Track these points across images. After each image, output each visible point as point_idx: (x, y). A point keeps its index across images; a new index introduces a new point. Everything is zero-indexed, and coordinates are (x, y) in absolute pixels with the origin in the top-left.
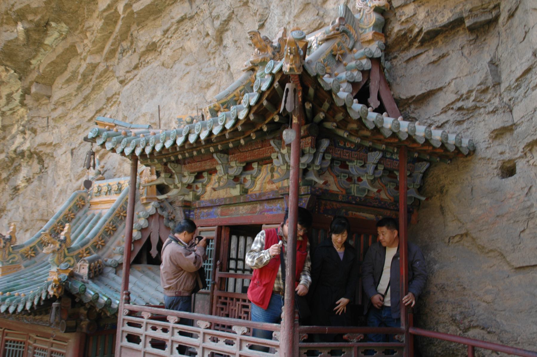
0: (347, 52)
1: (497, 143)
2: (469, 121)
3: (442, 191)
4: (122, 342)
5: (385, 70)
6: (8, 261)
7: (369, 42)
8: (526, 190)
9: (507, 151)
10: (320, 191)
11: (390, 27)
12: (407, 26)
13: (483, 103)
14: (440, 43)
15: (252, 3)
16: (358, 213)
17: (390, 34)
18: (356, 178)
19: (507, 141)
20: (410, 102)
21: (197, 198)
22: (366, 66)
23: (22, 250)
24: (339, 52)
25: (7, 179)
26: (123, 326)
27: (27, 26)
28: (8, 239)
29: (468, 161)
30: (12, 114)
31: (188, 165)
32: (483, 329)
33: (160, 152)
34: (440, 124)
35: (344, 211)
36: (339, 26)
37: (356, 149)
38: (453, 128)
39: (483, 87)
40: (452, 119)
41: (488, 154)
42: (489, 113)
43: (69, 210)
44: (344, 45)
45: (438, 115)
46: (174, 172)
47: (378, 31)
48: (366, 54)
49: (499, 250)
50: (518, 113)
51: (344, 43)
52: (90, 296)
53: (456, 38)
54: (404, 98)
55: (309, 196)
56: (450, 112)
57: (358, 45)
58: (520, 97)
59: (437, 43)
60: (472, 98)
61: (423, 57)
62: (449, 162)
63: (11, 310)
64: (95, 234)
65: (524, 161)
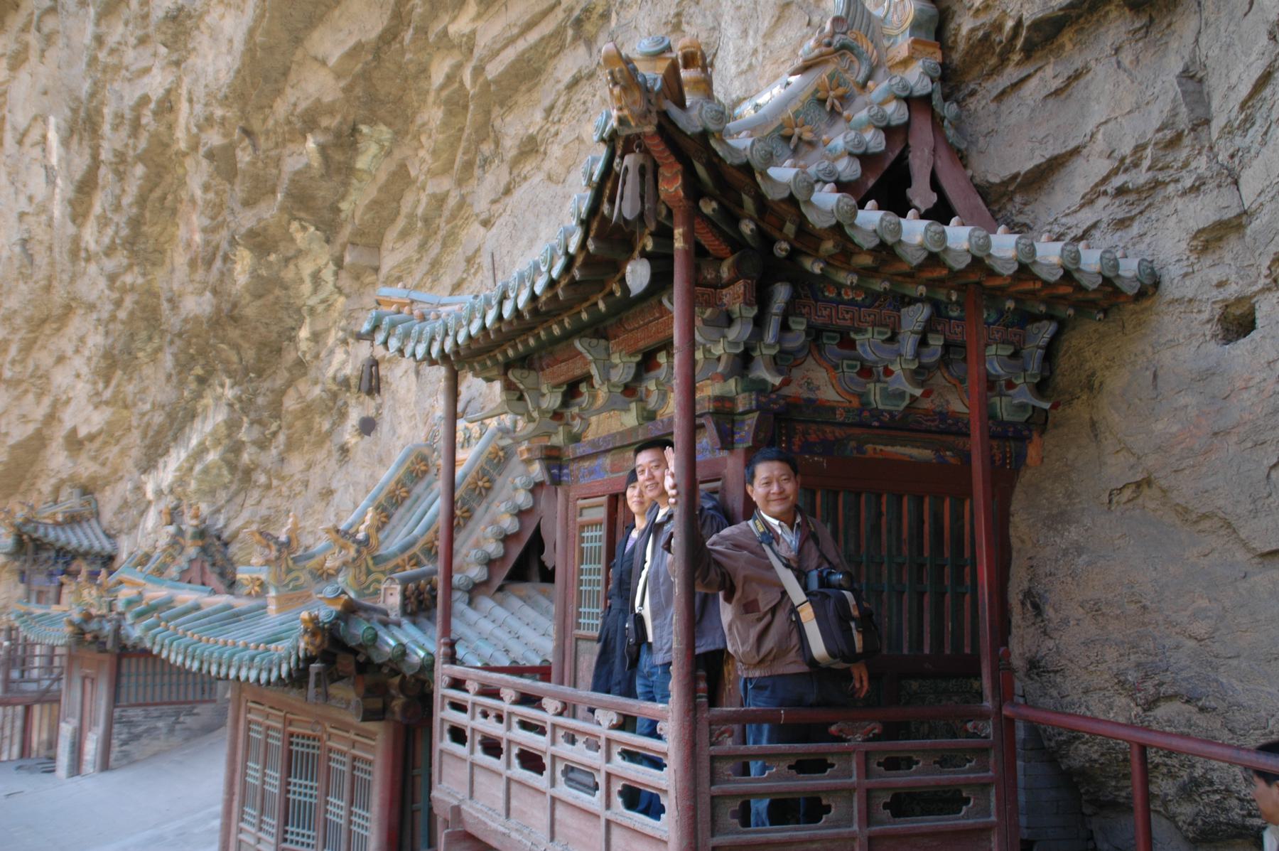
0: (856, 90)
1: (1209, 262)
2: (1143, 218)
3: (1091, 386)
5: (946, 123)
7: (905, 63)
9: (1233, 277)
10: (782, 402)
11: (952, 26)
12: (986, 19)
13: (1172, 171)
16: (889, 449)
17: (955, 42)
18: (881, 369)
19: (1231, 255)
20: (1011, 188)
21: (576, 439)
22: (895, 116)
24: (832, 93)
29: (1144, 311)
31: (548, 371)
33: (468, 347)
34: (1080, 232)
35: (853, 444)
36: (832, 36)
37: (868, 301)
38: (1108, 237)
39: (1169, 134)
40: (1105, 217)
41: (1189, 289)
42: (1184, 193)
44: (847, 76)
45: (1075, 212)
46: (522, 387)
47: (923, 39)
48: (894, 89)
50: (1251, 182)
51: (846, 71)
54: (996, 180)
55: (756, 415)
56: (1102, 201)
57: (880, 74)
58: (1256, 145)
60: (1146, 163)
62: (1101, 316)
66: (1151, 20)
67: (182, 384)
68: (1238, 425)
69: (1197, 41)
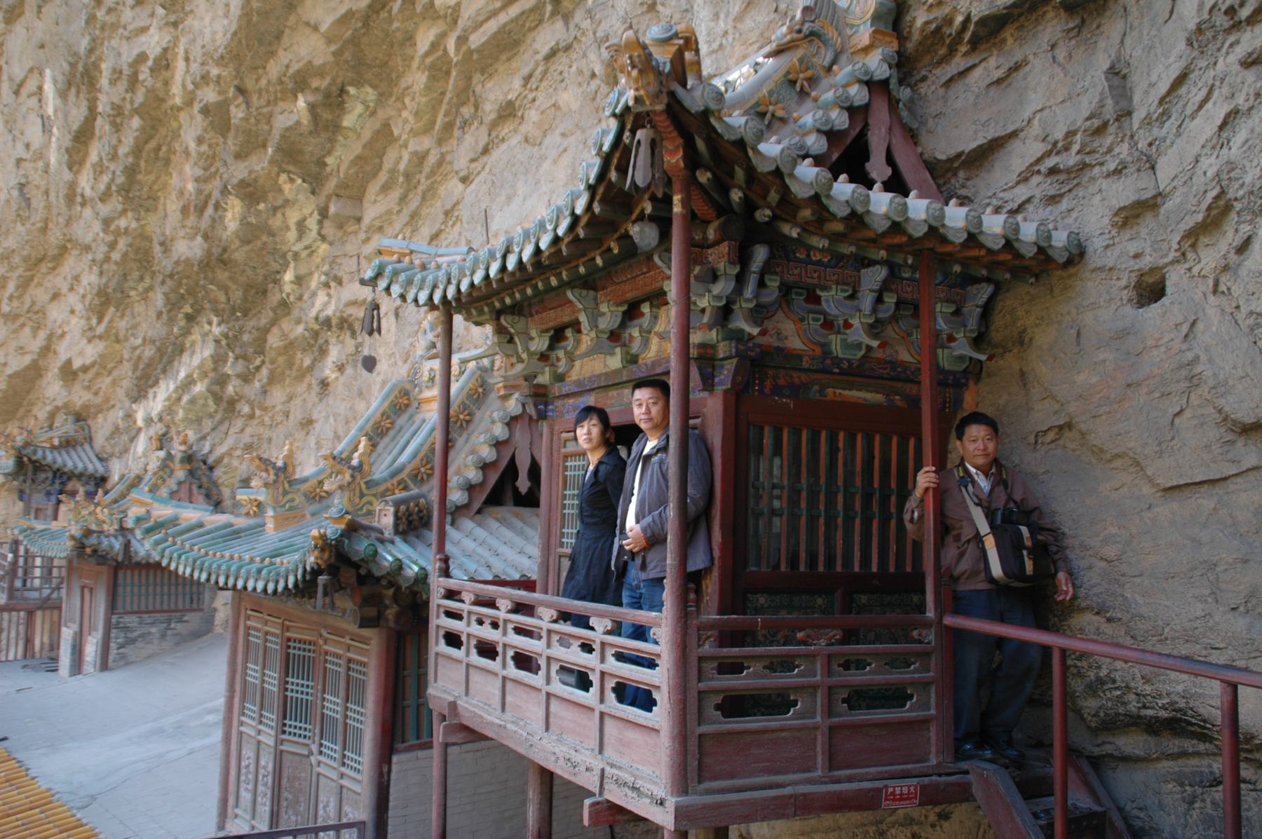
0: (822, 73)
1: (1128, 236)
2: (1072, 195)
3: (1021, 341)
4: (439, 647)
5: (901, 105)
6: (283, 506)
7: (866, 50)
8: (1185, 329)
9: (1148, 250)
11: (908, 18)
12: (939, 13)
13: (1097, 156)
14: (1010, 41)
15: (663, 5)
16: (846, 393)
17: (910, 32)
18: (841, 322)
19: (1146, 231)
20: (956, 165)
21: (560, 378)
22: (857, 98)
23: (305, 487)
24: (801, 76)
25: (311, 368)
26: (438, 617)
27: (311, 98)
28: (280, 469)
29: (1070, 276)
30: (310, 255)
31: (536, 317)
32: (1098, 613)
33: (470, 294)
34: (1015, 206)
35: (816, 388)
36: (802, 24)
37: (833, 262)
38: (1040, 211)
39: (1096, 123)
40: (1038, 193)
42: (1108, 176)
43: (383, 415)
44: (815, 60)
45: (1012, 188)
46: (512, 331)
47: (882, 29)
48: (857, 73)
49: (1131, 454)
50: (1166, 170)
51: (814, 56)
52: (386, 564)
53: (1040, 28)
54: (944, 157)
56: (1036, 179)
57: (843, 59)
58: (1171, 136)
59: (1004, 41)
60: (1076, 148)
61: (977, 72)
62: (1033, 280)
63: (271, 588)
64: (415, 455)
65: (1181, 268)
66: (1083, 21)
67: (171, 321)
68: (1148, 378)
69: (1122, 42)
